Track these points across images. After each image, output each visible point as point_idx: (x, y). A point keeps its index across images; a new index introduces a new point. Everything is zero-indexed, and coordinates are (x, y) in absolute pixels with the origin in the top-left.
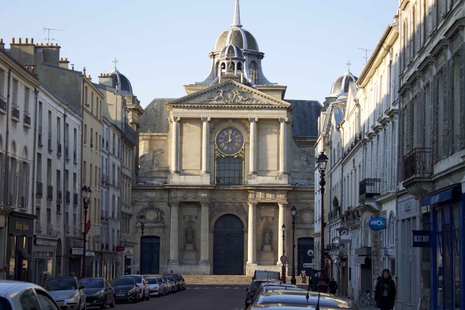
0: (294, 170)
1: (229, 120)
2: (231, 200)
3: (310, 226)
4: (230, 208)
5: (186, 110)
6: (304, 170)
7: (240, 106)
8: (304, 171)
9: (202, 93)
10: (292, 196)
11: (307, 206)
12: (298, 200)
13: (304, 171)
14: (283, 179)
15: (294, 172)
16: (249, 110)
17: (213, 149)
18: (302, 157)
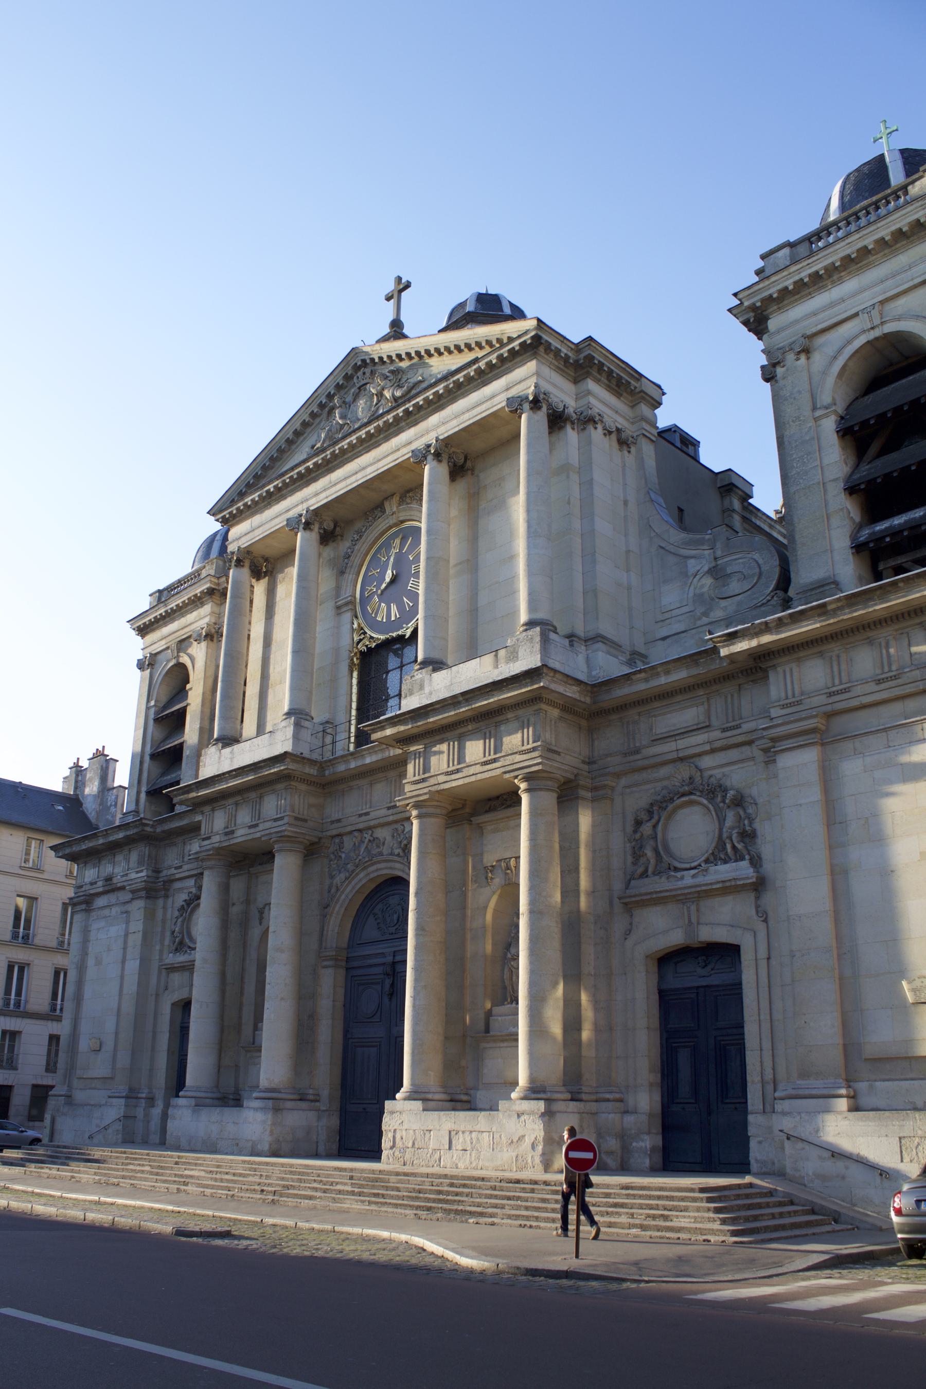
0: (664, 632)
1: (387, 505)
2: (384, 812)
3: (700, 880)
4: (385, 851)
5: (257, 519)
6: (705, 614)
7: (381, 423)
8: (705, 620)
9: (290, 442)
10: (611, 739)
11: (684, 771)
12: (637, 751)
13: (705, 620)
14: (521, 653)
15: (664, 639)
16: (416, 423)
17: (346, 628)
18: (691, 562)
